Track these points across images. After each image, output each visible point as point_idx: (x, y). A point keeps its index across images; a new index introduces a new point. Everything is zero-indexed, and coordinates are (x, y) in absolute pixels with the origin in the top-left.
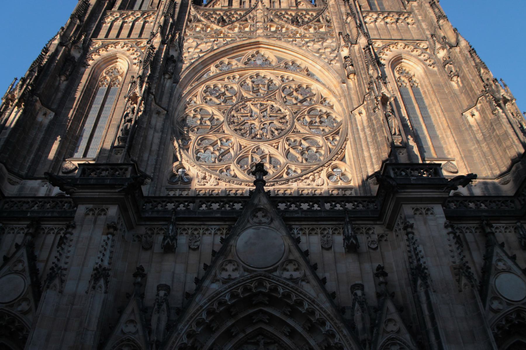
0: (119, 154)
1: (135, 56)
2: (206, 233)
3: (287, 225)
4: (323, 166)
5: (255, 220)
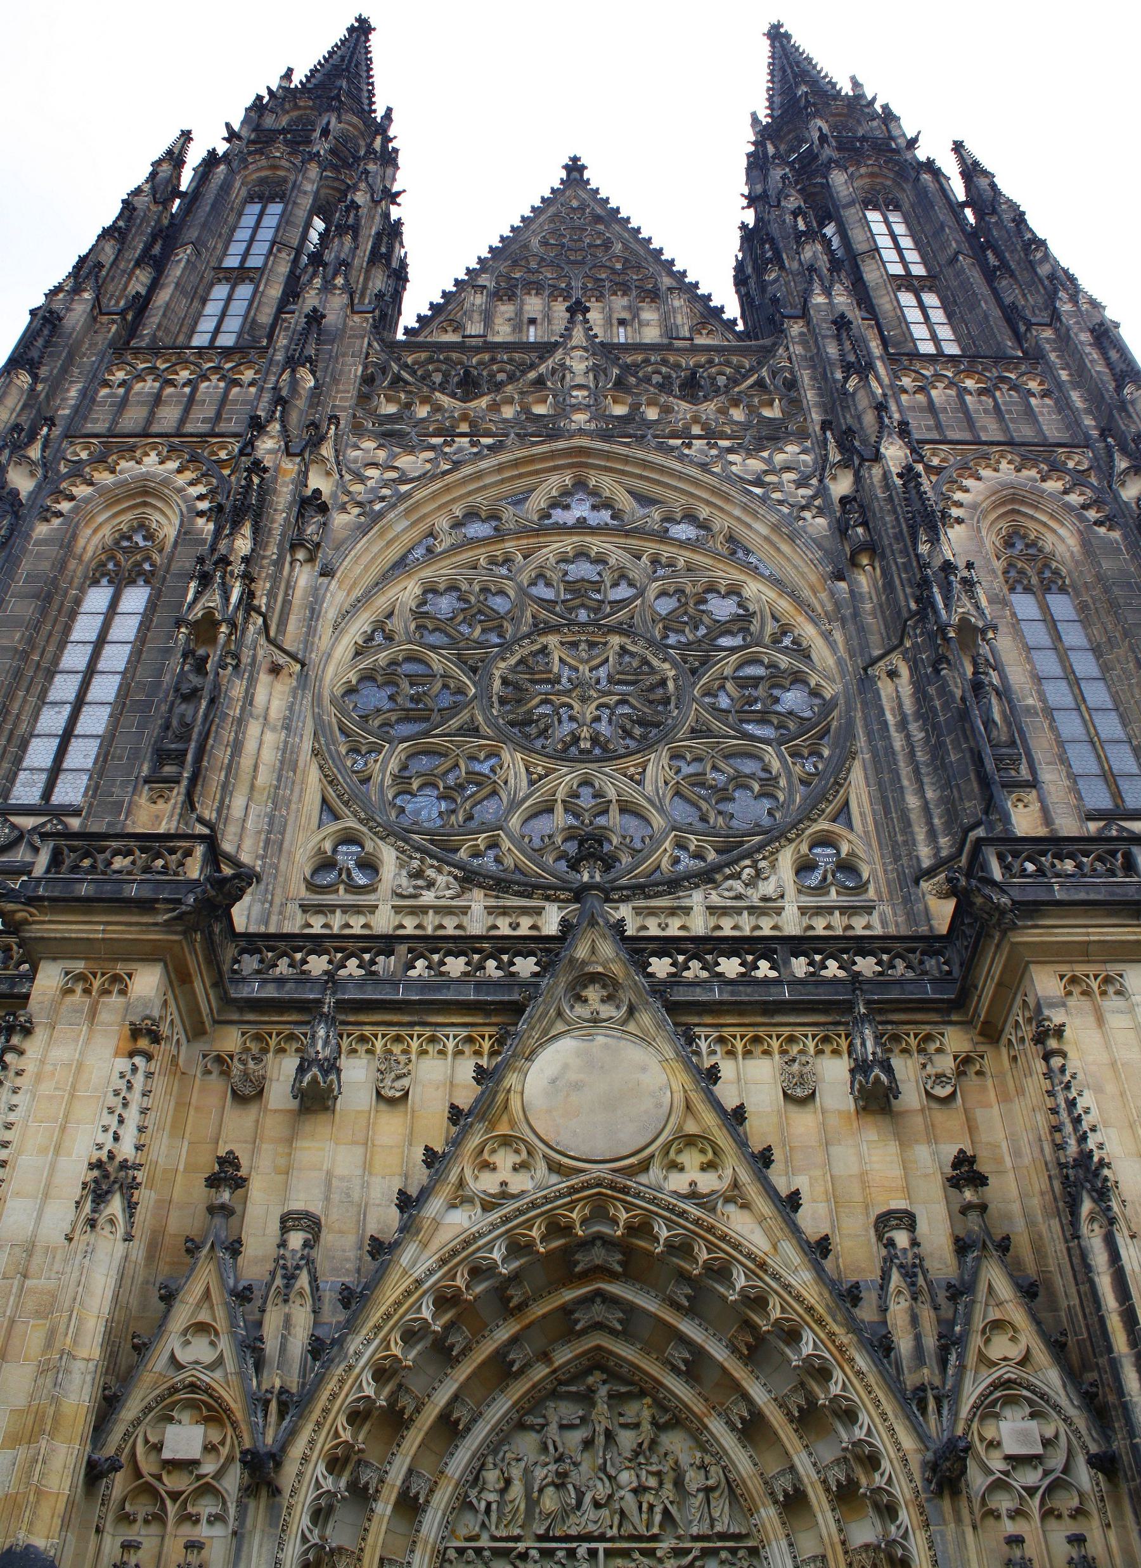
0: (161, 801)
1: (201, 489)
3: (676, 1024)
4: (783, 835)
5: (580, 1010)
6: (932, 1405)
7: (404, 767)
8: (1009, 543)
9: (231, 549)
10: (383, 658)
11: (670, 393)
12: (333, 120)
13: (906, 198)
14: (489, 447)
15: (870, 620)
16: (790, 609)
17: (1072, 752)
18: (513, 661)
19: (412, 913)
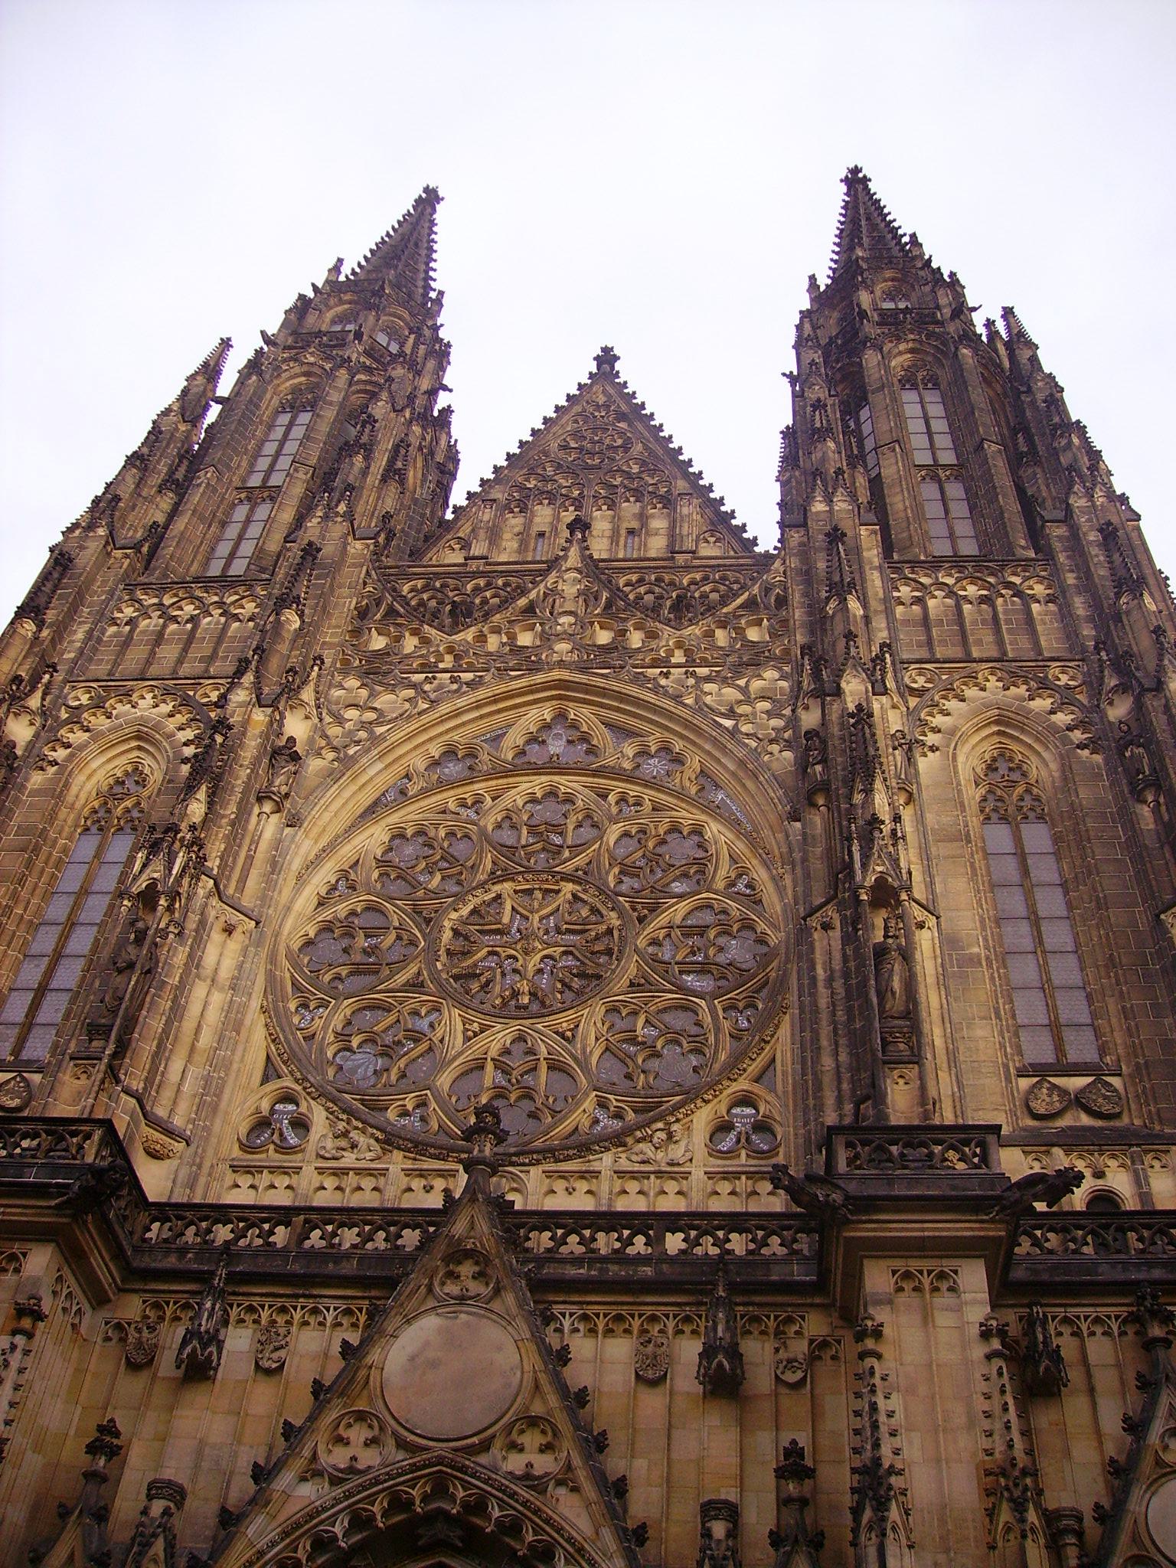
1: (189, 734)
2: (312, 1320)
5: (453, 1288)
7: (349, 1023)
8: (991, 768)
9: (184, 815)
10: (341, 909)
11: (657, 618)
12: (371, 319)
13: (945, 375)
15: (818, 867)
16: (746, 851)
17: (1019, 999)
18: (465, 911)
19: (334, 1174)
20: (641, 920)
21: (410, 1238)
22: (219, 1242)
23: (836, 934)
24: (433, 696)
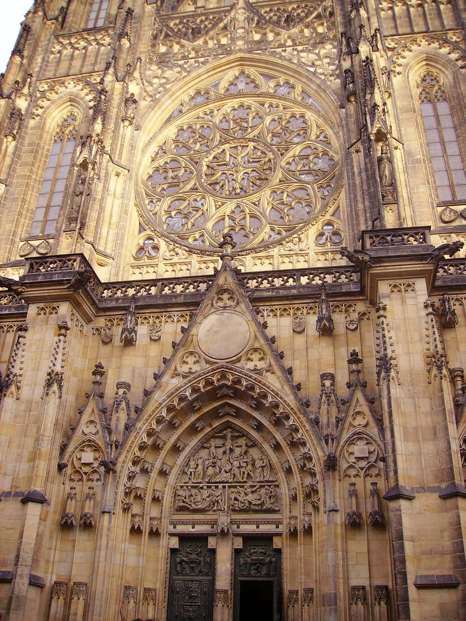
1: (90, 97)
5: (221, 304)
6: (330, 441)
8: (424, 80)
10: (161, 162)
11: (279, 26)
14: (202, 63)
15: (353, 127)
18: (211, 158)
20: (282, 155)
21: (203, 287)
22: (130, 295)
23: (362, 154)
24: (188, 69)
